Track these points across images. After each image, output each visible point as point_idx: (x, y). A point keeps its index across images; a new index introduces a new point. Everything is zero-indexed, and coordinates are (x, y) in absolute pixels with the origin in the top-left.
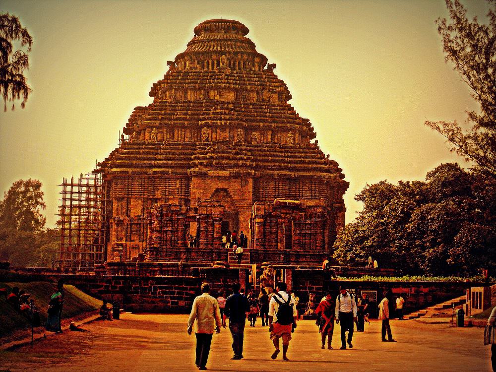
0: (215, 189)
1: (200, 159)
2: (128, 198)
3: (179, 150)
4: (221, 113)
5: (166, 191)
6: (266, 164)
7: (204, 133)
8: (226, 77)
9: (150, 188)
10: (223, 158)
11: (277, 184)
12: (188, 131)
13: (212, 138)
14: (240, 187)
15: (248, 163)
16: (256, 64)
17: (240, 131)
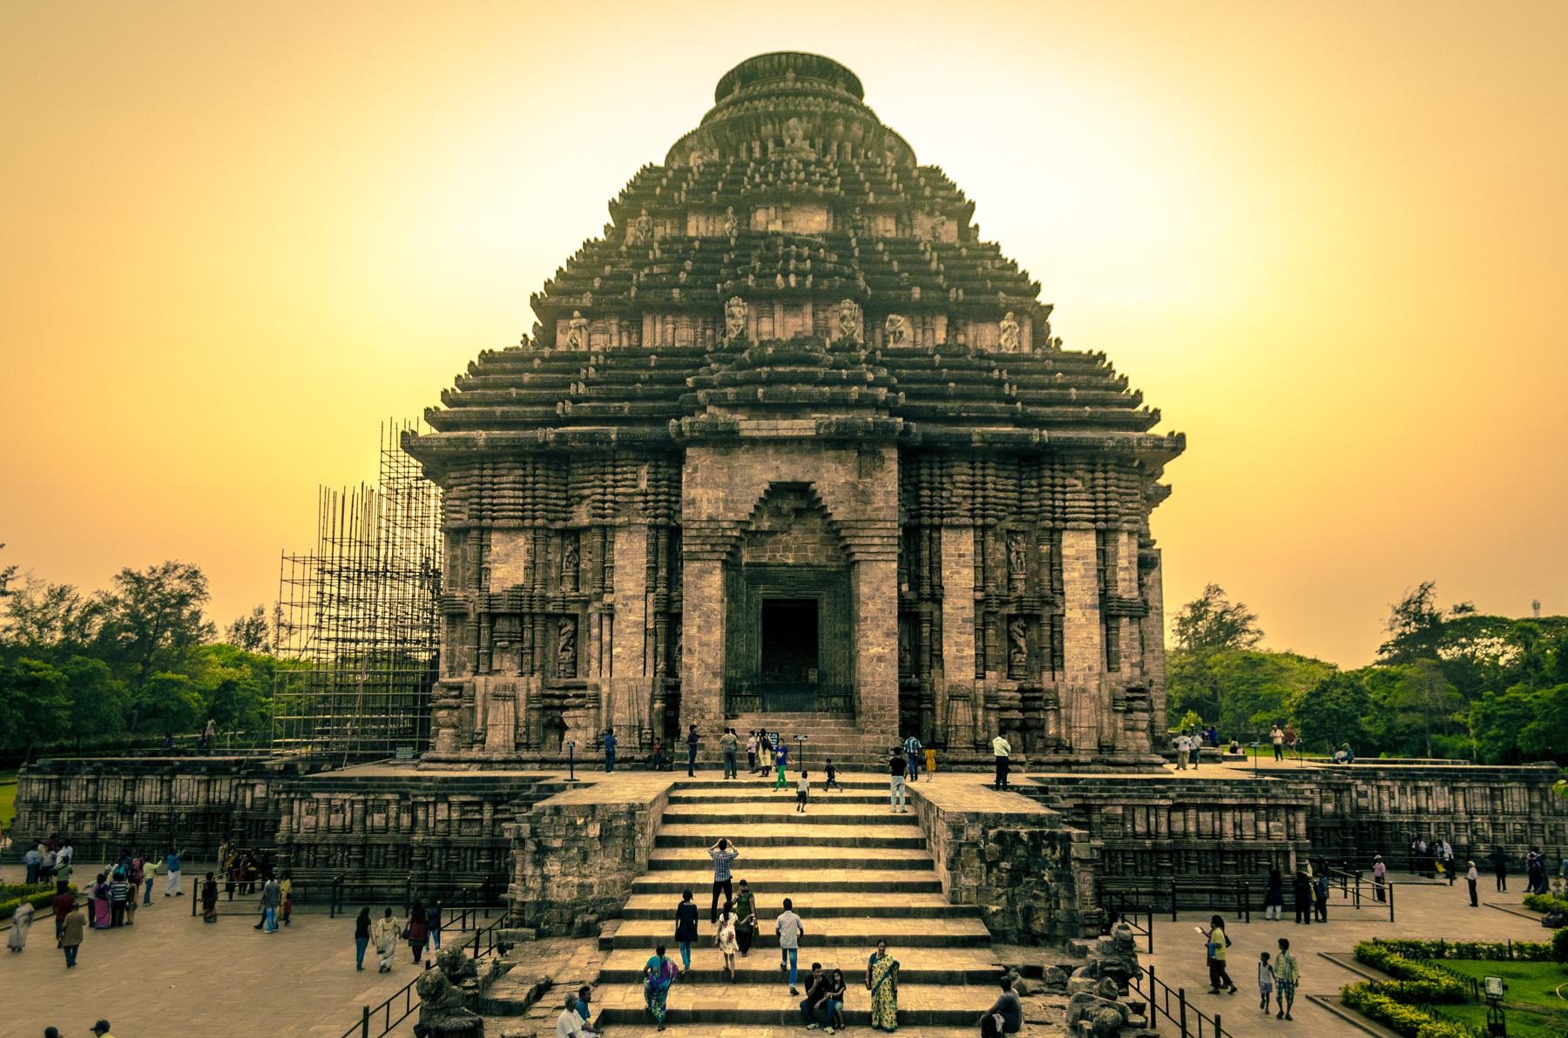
0: (766, 486)
1: (714, 388)
2: (482, 530)
3: (647, 368)
4: (787, 258)
5: (604, 502)
6: (940, 405)
7: (732, 316)
8: (801, 166)
9: (554, 495)
10: (792, 380)
11: (979, 472)
12: (685, 319)
13: (758, 334)
14: (852, 478)
15: (882, 393)
16: (888, 153)
17: (848, 307)
